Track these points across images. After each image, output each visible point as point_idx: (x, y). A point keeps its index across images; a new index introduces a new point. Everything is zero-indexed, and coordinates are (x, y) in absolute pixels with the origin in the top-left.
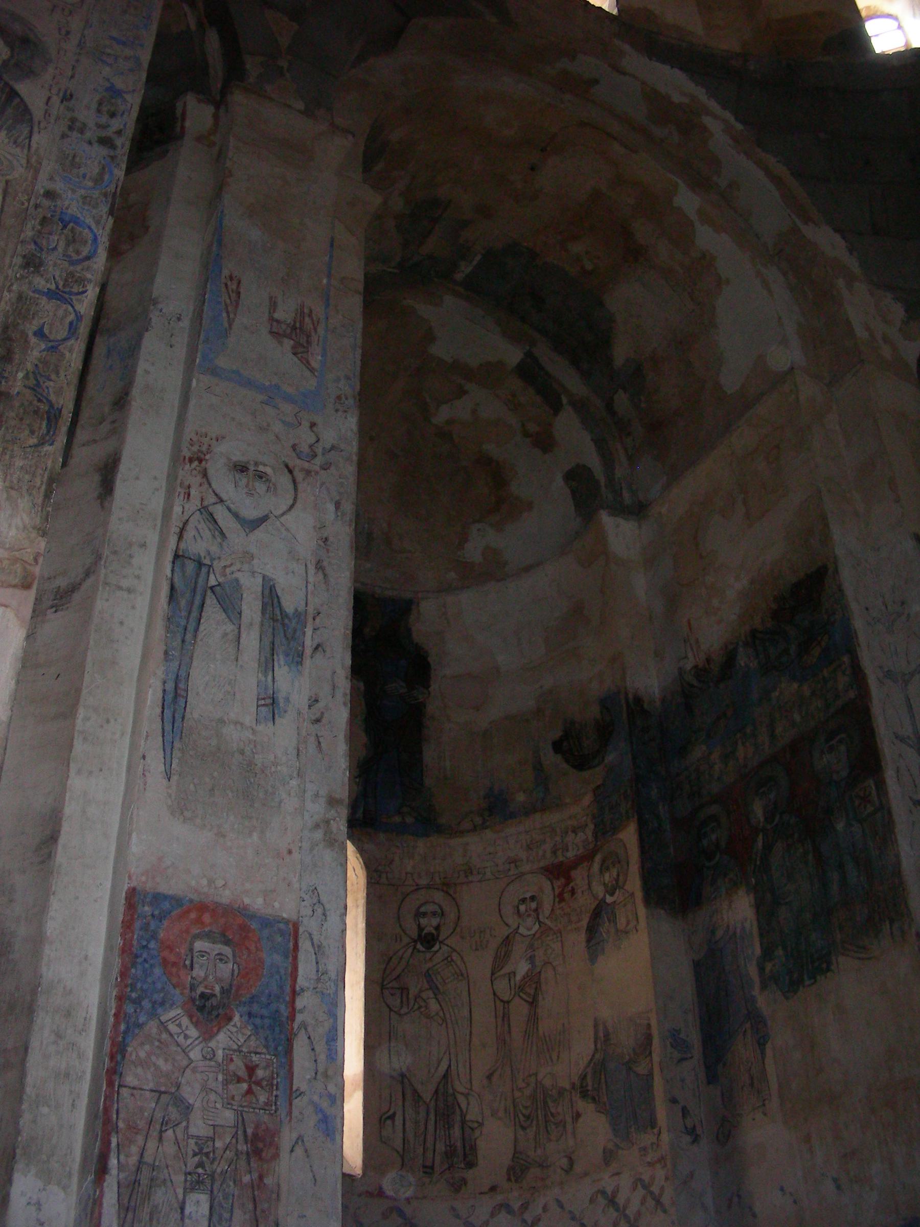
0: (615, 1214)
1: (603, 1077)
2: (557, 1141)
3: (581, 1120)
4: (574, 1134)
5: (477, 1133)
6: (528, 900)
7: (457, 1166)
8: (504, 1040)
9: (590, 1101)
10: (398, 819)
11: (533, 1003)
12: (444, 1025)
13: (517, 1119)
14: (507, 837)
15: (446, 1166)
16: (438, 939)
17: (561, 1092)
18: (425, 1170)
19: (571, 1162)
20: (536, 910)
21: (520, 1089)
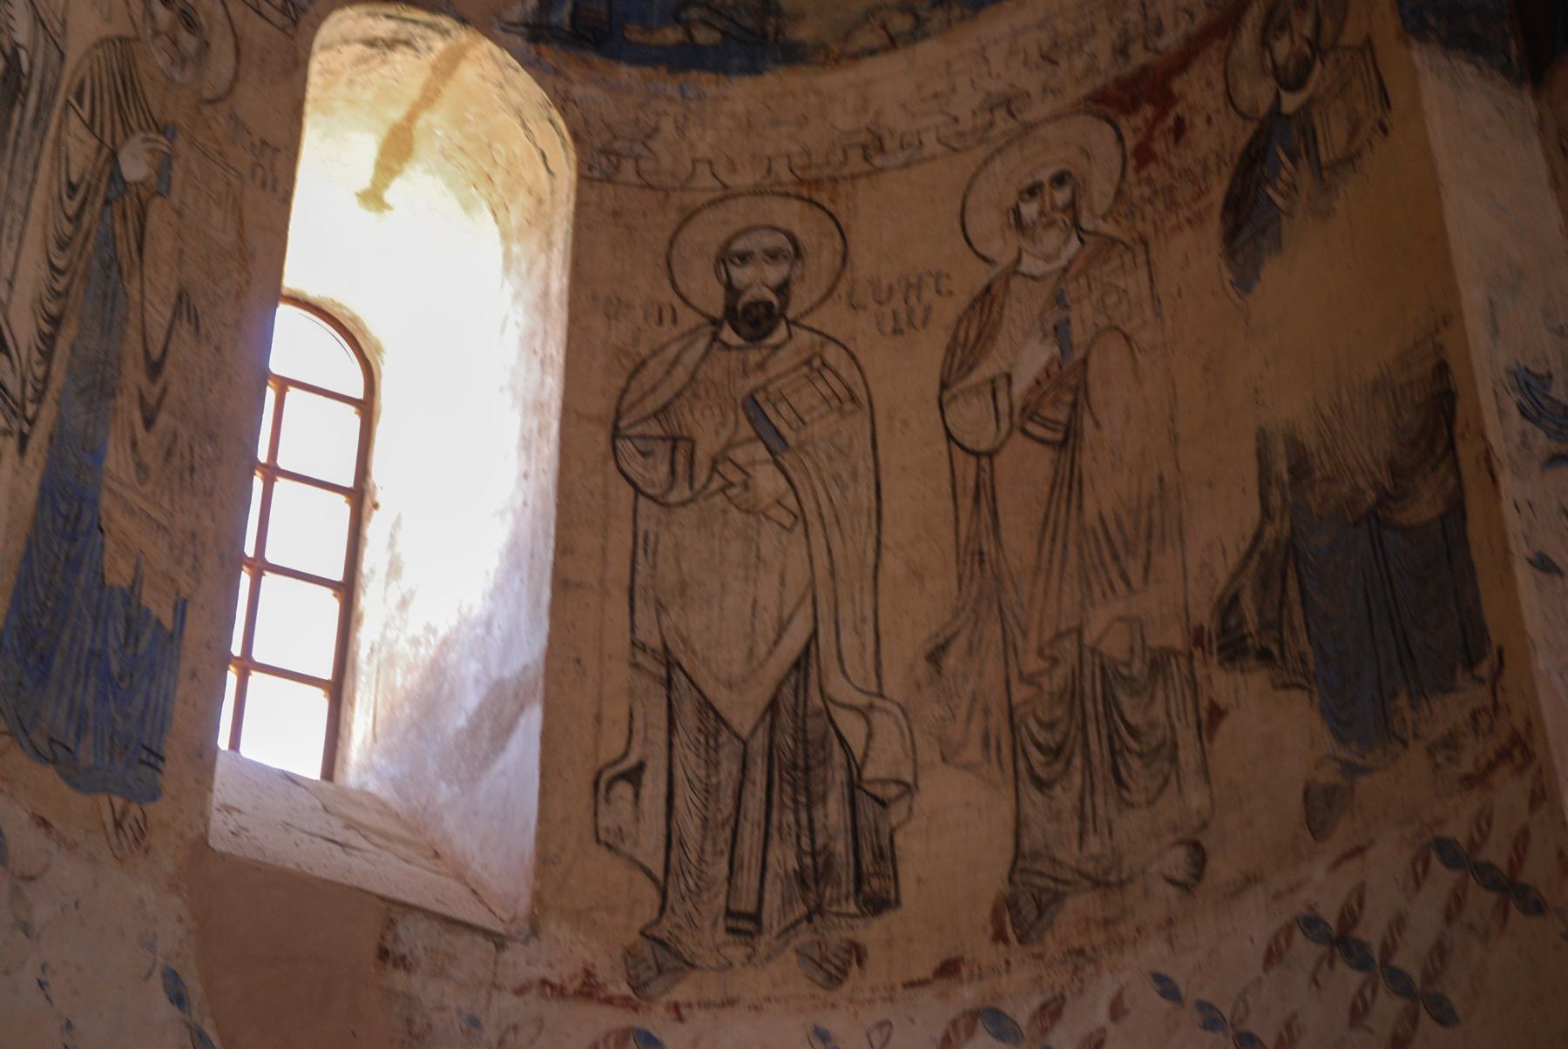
0: (1355, 978)
1: (1292, 584)
2: (1150, 803)
3: (1225, 726)
4: (1205, 772)
5: (897, 814)
6: (1047, 188)
7: (835, 908)
8: (981, 553)
9: (1252, 662)
10: (672, 35)
11: (1067, 441)
12: (799, 529)
13: (1022, 764)
14: (984, 49)
15: (800, 909)
16: (783, 315)
17: (1159, 663)
18: (731, 923)
19: (1199, 856)
20: (1072, 207)
21: (1029, 680)
